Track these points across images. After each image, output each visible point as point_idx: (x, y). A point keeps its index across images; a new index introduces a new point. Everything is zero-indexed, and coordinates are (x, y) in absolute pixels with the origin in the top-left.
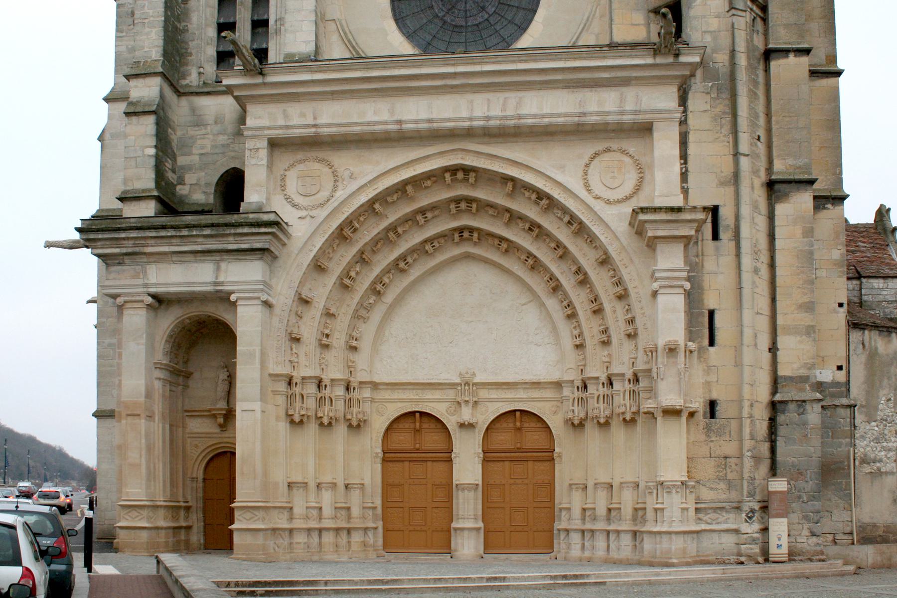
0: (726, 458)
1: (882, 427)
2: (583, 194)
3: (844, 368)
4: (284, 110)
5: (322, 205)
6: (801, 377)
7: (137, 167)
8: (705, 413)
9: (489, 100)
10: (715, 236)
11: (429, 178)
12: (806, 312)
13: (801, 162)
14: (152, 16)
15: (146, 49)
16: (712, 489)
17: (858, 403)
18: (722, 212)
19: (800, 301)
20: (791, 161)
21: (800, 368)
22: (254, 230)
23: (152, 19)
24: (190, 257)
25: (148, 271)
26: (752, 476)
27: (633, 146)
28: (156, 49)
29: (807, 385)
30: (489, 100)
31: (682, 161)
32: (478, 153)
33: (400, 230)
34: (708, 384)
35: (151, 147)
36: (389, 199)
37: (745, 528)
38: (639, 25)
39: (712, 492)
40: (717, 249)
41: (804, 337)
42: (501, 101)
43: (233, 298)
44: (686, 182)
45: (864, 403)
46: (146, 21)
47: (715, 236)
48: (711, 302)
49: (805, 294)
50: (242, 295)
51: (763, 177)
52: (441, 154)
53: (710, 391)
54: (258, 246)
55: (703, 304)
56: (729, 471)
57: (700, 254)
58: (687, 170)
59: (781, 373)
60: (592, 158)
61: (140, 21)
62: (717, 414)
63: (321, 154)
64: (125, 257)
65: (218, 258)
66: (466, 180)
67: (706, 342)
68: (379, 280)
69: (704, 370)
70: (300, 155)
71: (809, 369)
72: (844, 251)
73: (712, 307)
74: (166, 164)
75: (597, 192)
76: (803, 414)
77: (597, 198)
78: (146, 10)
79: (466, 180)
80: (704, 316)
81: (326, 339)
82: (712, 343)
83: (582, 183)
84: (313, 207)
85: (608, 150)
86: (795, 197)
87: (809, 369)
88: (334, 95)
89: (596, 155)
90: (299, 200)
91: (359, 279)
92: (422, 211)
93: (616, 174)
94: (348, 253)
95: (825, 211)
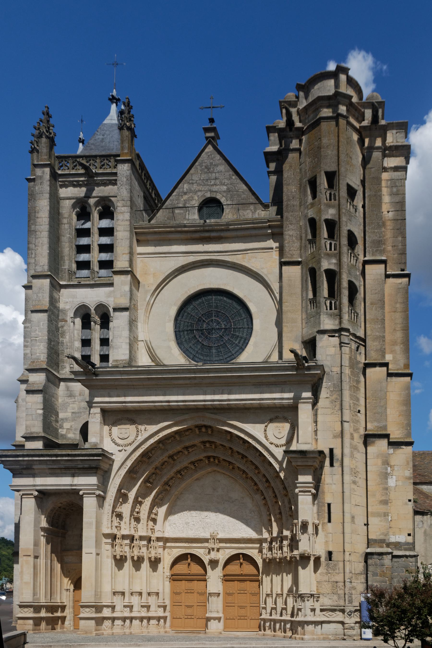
0: (337, 582)
2: (264, 441)
6: (381, 540)
7: (33, 420)
8: (326, 558)
10: (332, 465)
13: (381, 424)
14: (41, 336)
15: (38, 355)
16: (330, 599)
17: (419, 554)
19: (381, 499)
20: (376, 424)
21: (380, 535)
26: (350, 592)
28: (43, 355)
29: (384, 544)
34: (327, 542)
35: (40, 409)
37: (347, 620)
39: (330, 601)
41: (383, 518)
44: (317, 436)
47: (332, 465)
48: (328, 499)
49: (383, 495)
51: (362, 432)
55: (324, 500)
56: (338, 589)
59: (369, 537)
61: (34, 338)
62: (333, 559)
67: (326, 520)
69: (325, 535)
72: (411, 471)
73: (329, 502)
75: (271, 440)
76: (381, 559)
77: (271, 443)
78: (37, 332)
79: (207, 432)
80: (325, 507)
82: (329, 521)
83: (264, 435)
87: (386, 535)
93: (281, 431)
95: (401, 450)
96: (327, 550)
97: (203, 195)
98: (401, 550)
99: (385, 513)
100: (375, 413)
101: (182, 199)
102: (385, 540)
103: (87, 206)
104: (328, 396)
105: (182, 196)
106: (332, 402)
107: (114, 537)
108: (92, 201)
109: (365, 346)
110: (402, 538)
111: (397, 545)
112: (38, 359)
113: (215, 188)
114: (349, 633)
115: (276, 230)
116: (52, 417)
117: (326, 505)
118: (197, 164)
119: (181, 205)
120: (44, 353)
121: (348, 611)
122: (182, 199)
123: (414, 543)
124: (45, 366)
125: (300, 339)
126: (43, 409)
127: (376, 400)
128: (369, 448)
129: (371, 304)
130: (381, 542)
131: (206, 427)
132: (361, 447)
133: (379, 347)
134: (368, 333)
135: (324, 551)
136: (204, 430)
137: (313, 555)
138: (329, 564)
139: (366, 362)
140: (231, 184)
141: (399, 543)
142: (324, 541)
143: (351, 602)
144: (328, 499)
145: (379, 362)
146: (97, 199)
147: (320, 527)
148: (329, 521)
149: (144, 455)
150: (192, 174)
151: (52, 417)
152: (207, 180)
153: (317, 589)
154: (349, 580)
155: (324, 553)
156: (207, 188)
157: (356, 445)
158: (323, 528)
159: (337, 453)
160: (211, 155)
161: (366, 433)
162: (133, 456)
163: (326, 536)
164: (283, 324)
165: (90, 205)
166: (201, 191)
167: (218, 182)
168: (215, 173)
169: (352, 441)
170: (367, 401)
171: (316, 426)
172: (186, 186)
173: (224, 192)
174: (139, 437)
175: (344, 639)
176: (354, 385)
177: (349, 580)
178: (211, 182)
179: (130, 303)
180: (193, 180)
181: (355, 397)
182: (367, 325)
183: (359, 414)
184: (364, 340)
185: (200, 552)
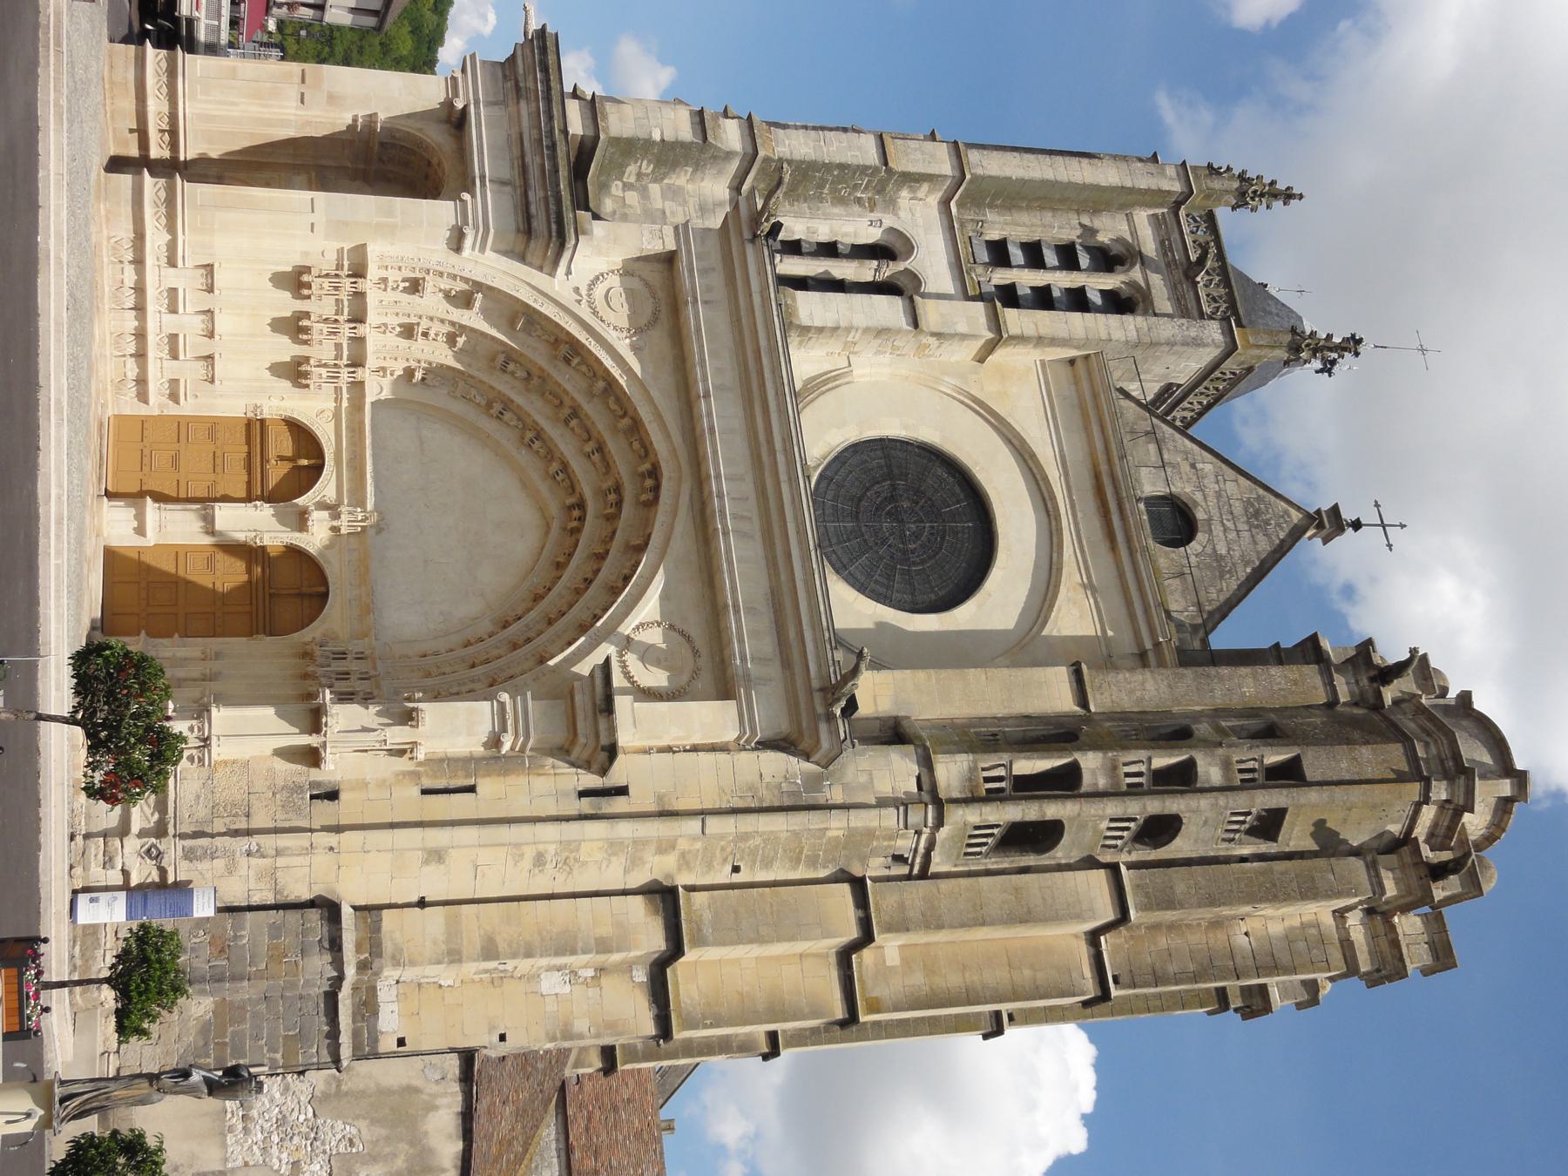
1: (304, 1129)
3: (401, 1049)
4: (713, 269)
5: (595, 313)
6: (379, 945)
7: (635, 119)
9: (747, 499)
10: (583, 794)
11: (644, 446)
12: (483, 948)
15: (787, 142)
16: (198, 797)
17: (343, 1076)
18: (622, 799)
19: (498, 939)
22: (553, 217)
23: (825, 149)
24: (516, 152)
25: (496, 107)
26: (218, 854)
27: (705, 681)
29: (367, 955)
30: (747, 499)
31: (688, 748)
32: (677, 497)
33: (574, 423)
34: (364, 785)
35: (662, 134)
36: (611, 400)
38: (876, 704)
39: (192, 797)
40: (566, 794)
42: (745, 514)
43: (466, 196)
44: (658, 752)
45: (344, 1088)
46: (822, 143)
47: (583, 794)
48: (486, 786)
49: (510, 946)
50: (469, 206)
51: (682, 880)
52: (674, 451)
53: (353, 789)
54: (535, 224)
55: (484, 776)
57: (558, 771)
58: (674, 752)
59: (385, 912)
60: (682, 633)
63: (664, 315)
64: (513, 82)
65: (518, 184)
66: (644, 490)
67: (428, 783)
68: (507, 405)
69: (384, 781)
70: (661, 294)
71: (393, 957)
74: (645, 162)
79: (644, 490)
81: (420, 331)
82: (425, 792)
84: (590, 304)
85: (696, 653)
86: (655, 923)
87: (393, 957)
88: (736, 321)
89: (688, 638)
90: (599, 291)
91: (507, 377)
92: (600, 448)
94: (539, 356)
96: (341, 787)
97: (1196, 503)
98: (354, 1022)
99: (459, 953)
100: (736, 912)
101: (1179, 459)
102: (380, 955)
103: (1126, 267)
104: (767, 779)
105: (1187, 459)
106: (751, 788)
107: (358, 272)
108: (1136, 274)
109: (909, 877)
110: (390, 1022)
111: (368, 1007)
112: (777, 142)
113: (1217, 529)
114: (93, 852)
115: (1151, 657)
116: (648, 166)
117: (471, 782)
118: (1261, 491)
119: (1166, 456)
120: (791, 153)
121: (161, 848)
122: (1179, 459)
123: (377, 1056)
124: (762, 153)
125: (902, 714)
126: (663, 140)
127: (772, 913)
128: (639, 899)
129: (1016, 889)
130: (373, 945)
131: (656, 489)
132: (638, 879)
133: (911, 914)
134: (944, 885)
135: (338, 778)
136: (649, 483)
137: (325, 743)
138: (302, 792)
139: (869, 882)
140: (1233, 564)
141: (375, 1013)
142: (368, 778)
143: (189, 855)
144: (486, 786)
145: (873, 915)
146: (1143, 285)
147: (402, 764)
148: (425, 792)
149: (575, 347)
150: (1236, 481)
151: (648, 166)
152: (1232, 513)
153: (225, 762)
154: (254, 848)
155: (332, 780)
156: (1215, 512)
157: (644, 863)
158: (405, 774)
159: (619, 805)
160: (1286, 522)
161: (680, 889)
162: (567, 318)
163: (382, 784)
164: (932, 671)
165: (1128, 270)
166: (1205, 498)
167: (1232, 535)
168: (1250, 530)
169: (653, 848)
170: (767, 890)
171: (685, 751)
172: (1208, 468)
173: (1214, 550)
174: (614, 334)
175: (72, 837)
176: (803, 848)
177: (254, 848)
178: (1228, 520)
179: (933, 334)
180: (1225, 481)
181: (772, 854)
182: (963, 881)
183: (730, 868)
184: (924, 875)
185: (326, 487)
